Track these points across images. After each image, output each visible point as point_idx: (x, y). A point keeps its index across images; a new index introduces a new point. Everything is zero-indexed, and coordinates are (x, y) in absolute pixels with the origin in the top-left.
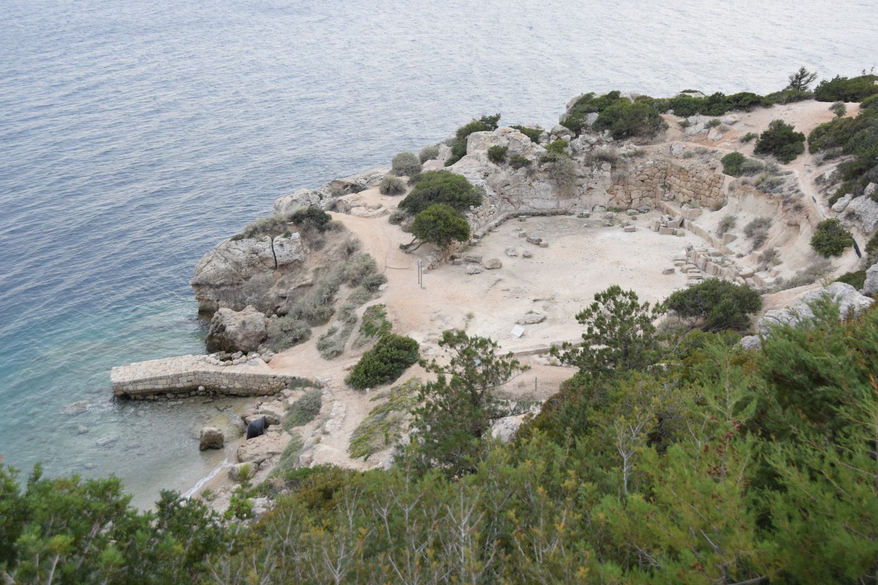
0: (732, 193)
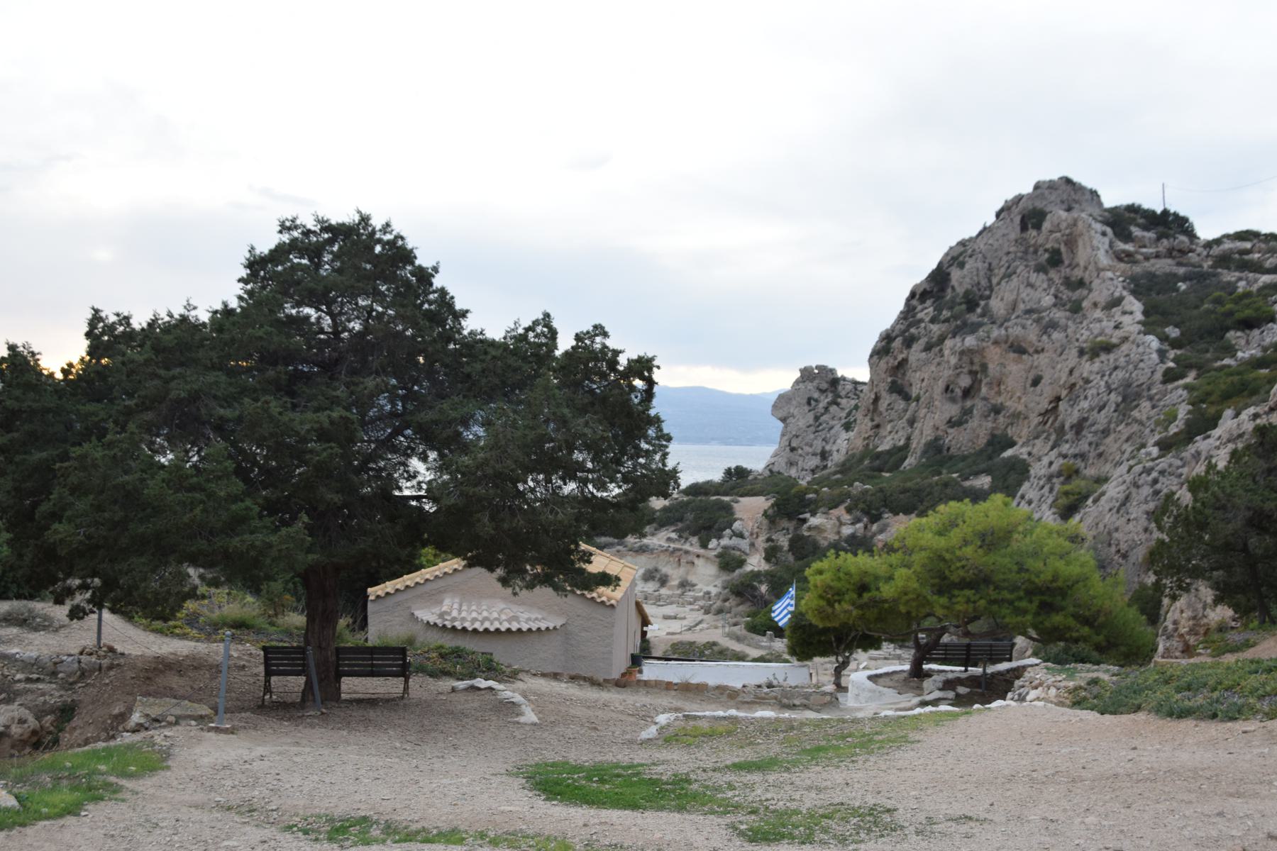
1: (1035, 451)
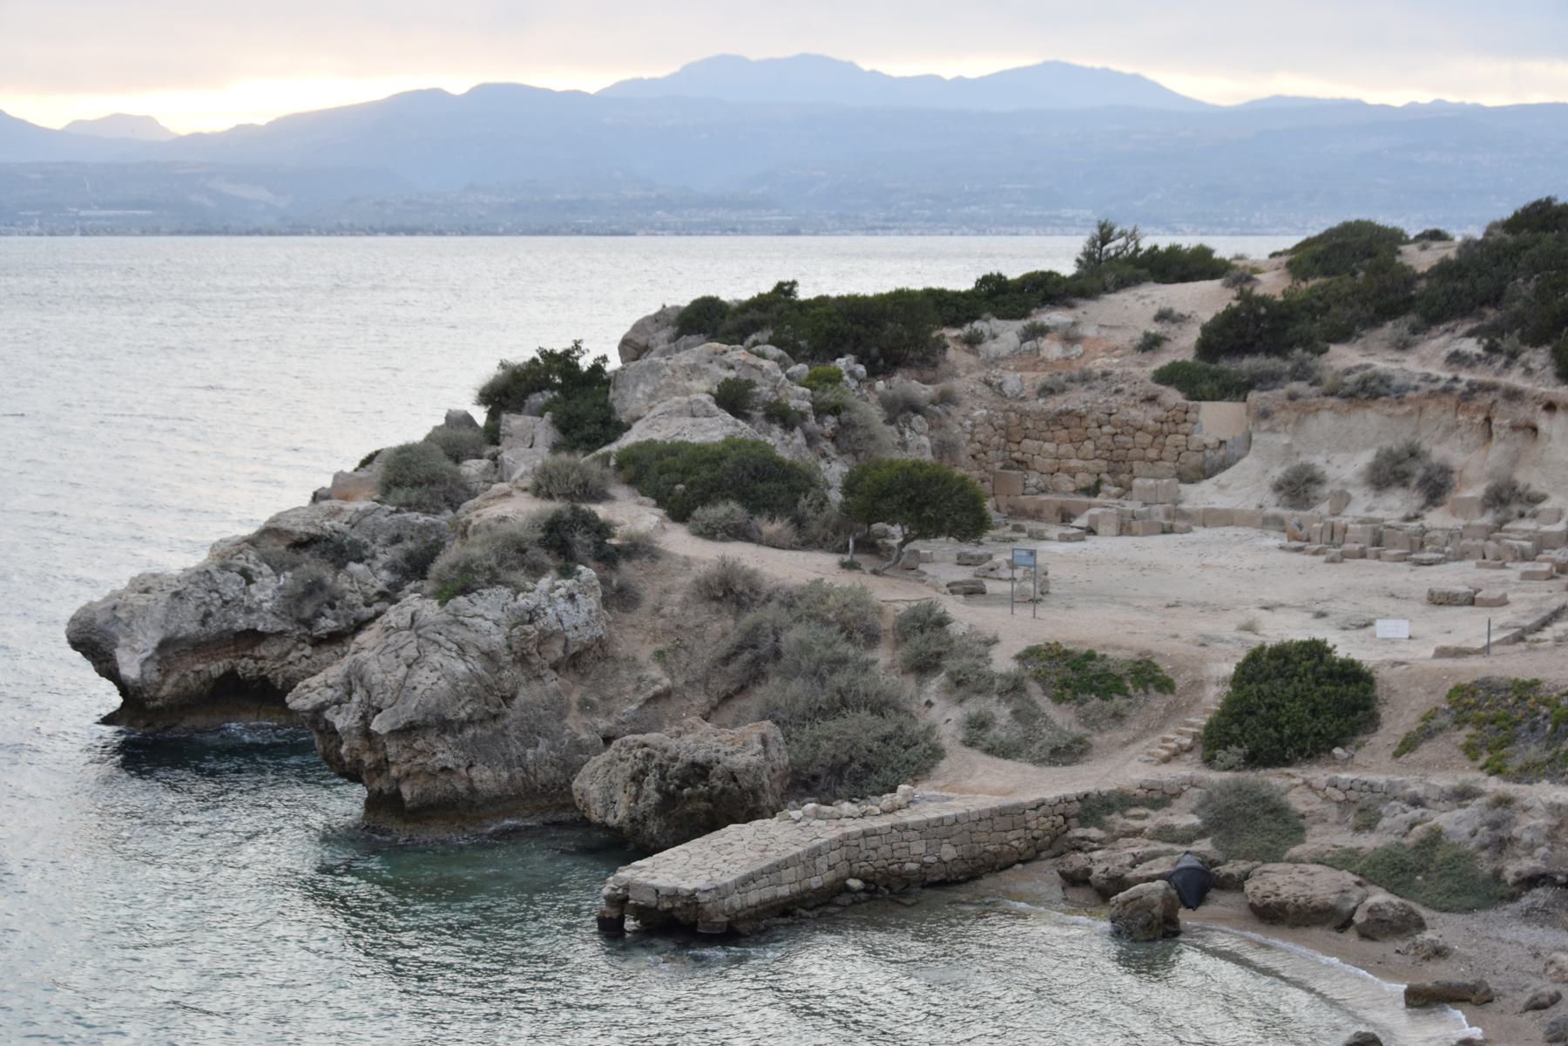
0: (1265, 425)
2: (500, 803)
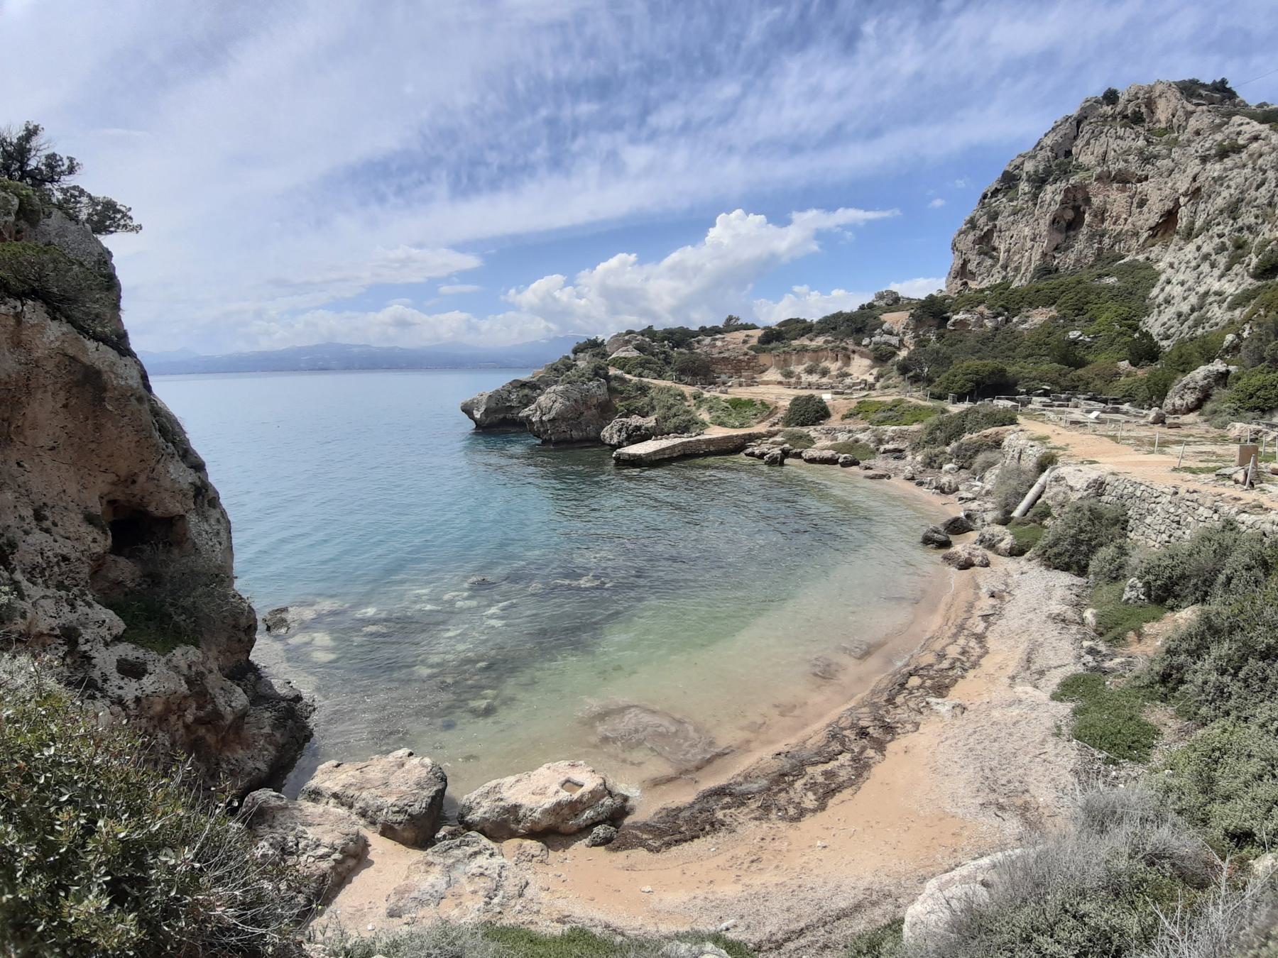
1: (1152, 256)
2: (581, 441)
